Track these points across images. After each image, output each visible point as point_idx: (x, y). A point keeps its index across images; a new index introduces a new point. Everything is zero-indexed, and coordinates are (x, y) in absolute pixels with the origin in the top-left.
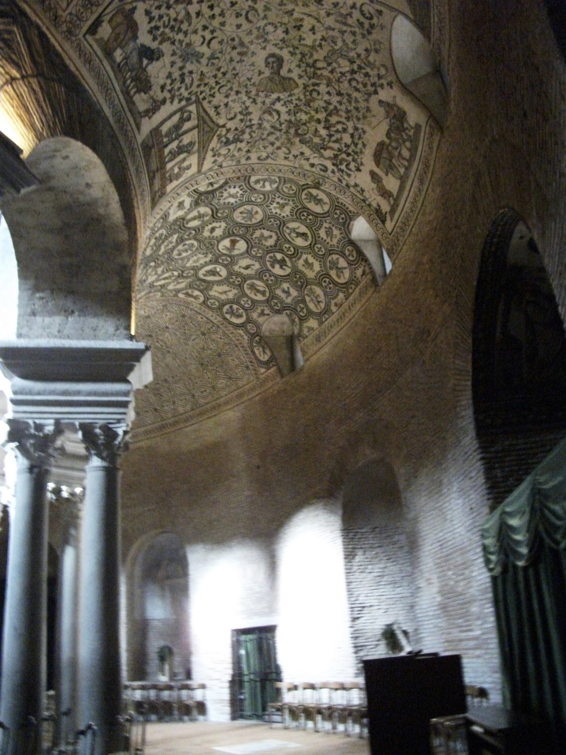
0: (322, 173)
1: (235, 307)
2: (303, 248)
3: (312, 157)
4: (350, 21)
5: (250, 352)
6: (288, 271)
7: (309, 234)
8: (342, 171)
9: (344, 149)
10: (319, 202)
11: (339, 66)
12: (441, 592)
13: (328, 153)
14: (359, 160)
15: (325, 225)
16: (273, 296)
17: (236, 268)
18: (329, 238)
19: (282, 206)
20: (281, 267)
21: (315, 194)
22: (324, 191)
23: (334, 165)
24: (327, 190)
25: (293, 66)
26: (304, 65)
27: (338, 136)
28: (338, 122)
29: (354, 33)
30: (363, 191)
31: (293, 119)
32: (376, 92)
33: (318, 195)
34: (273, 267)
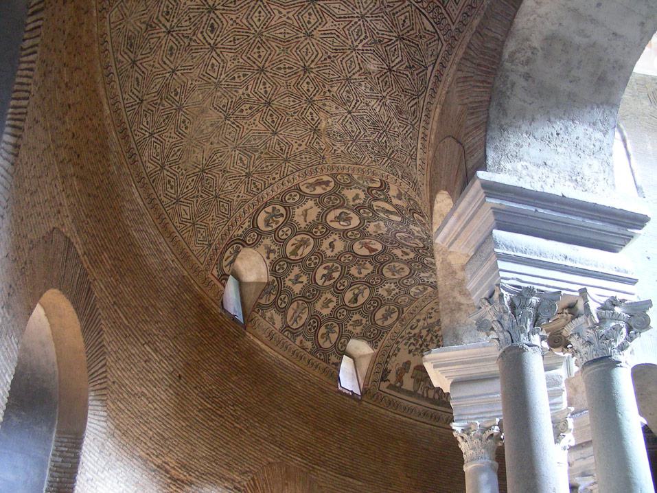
0: (410, 326)
1: (281, 220)
2: (343, 298)
5: (225, 242)
6: (320, 282)
7: (355, 305)
8: (409, 340)
9: (425, 344)
10: (385, 318)
13: (424, 333)
14: (416, 353)
15: (364, 321)
16: (291, 263)
17: (336, 237)
18: (352, 323)
19: (389, 291)
20: (324, 275)
21: (392, 316)
22: (394, 323)
23: (415, 335)
27: (435, 341)
30: (396, 355)
34: (325, 268)
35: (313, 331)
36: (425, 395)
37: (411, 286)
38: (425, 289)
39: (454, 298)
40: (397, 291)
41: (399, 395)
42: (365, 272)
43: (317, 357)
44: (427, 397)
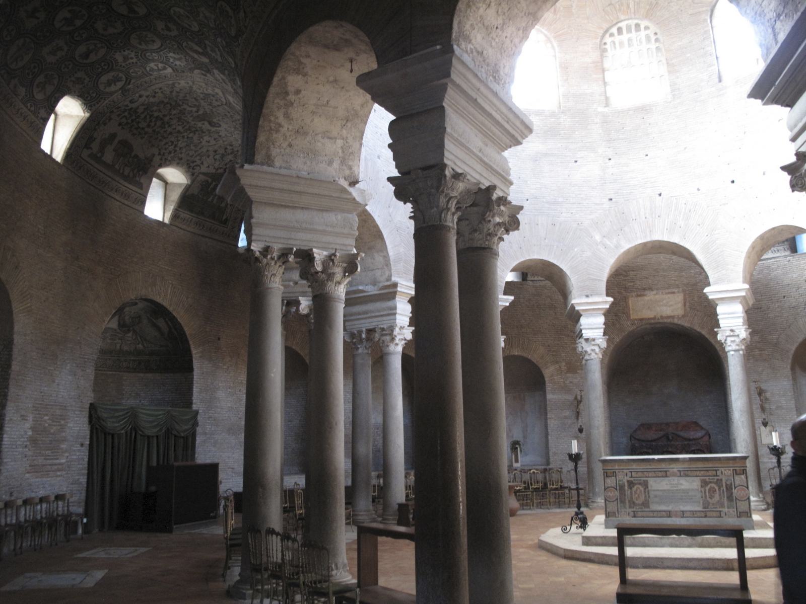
3: (147, 99)
4: (198, 158)
7: (85, 61)
8: (124, 112)
10: (109, 84)
11: (183, 142)
12: (33, 428)
21: (117, 83)
23: (131, 108)
24: (116, 94)
25: (204, 126)
26: (199, 129)
27: (148, 120)
28: (155, 124)
29: (192, 156)
30: (105, 124)
31: (179, 108)
32: (159, 154)
33: (115, 85)
35: (31, 77)
36: (121, 172)
37: (153, 60)
38: (165, 68)
39: (277, 118)
40: (134, 60)
41: (96, 165)
42: (111, 30)
43: (27, 107)
44: (123, 173)
